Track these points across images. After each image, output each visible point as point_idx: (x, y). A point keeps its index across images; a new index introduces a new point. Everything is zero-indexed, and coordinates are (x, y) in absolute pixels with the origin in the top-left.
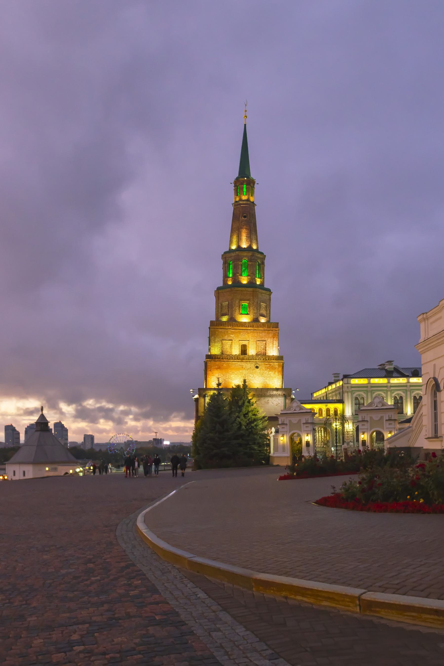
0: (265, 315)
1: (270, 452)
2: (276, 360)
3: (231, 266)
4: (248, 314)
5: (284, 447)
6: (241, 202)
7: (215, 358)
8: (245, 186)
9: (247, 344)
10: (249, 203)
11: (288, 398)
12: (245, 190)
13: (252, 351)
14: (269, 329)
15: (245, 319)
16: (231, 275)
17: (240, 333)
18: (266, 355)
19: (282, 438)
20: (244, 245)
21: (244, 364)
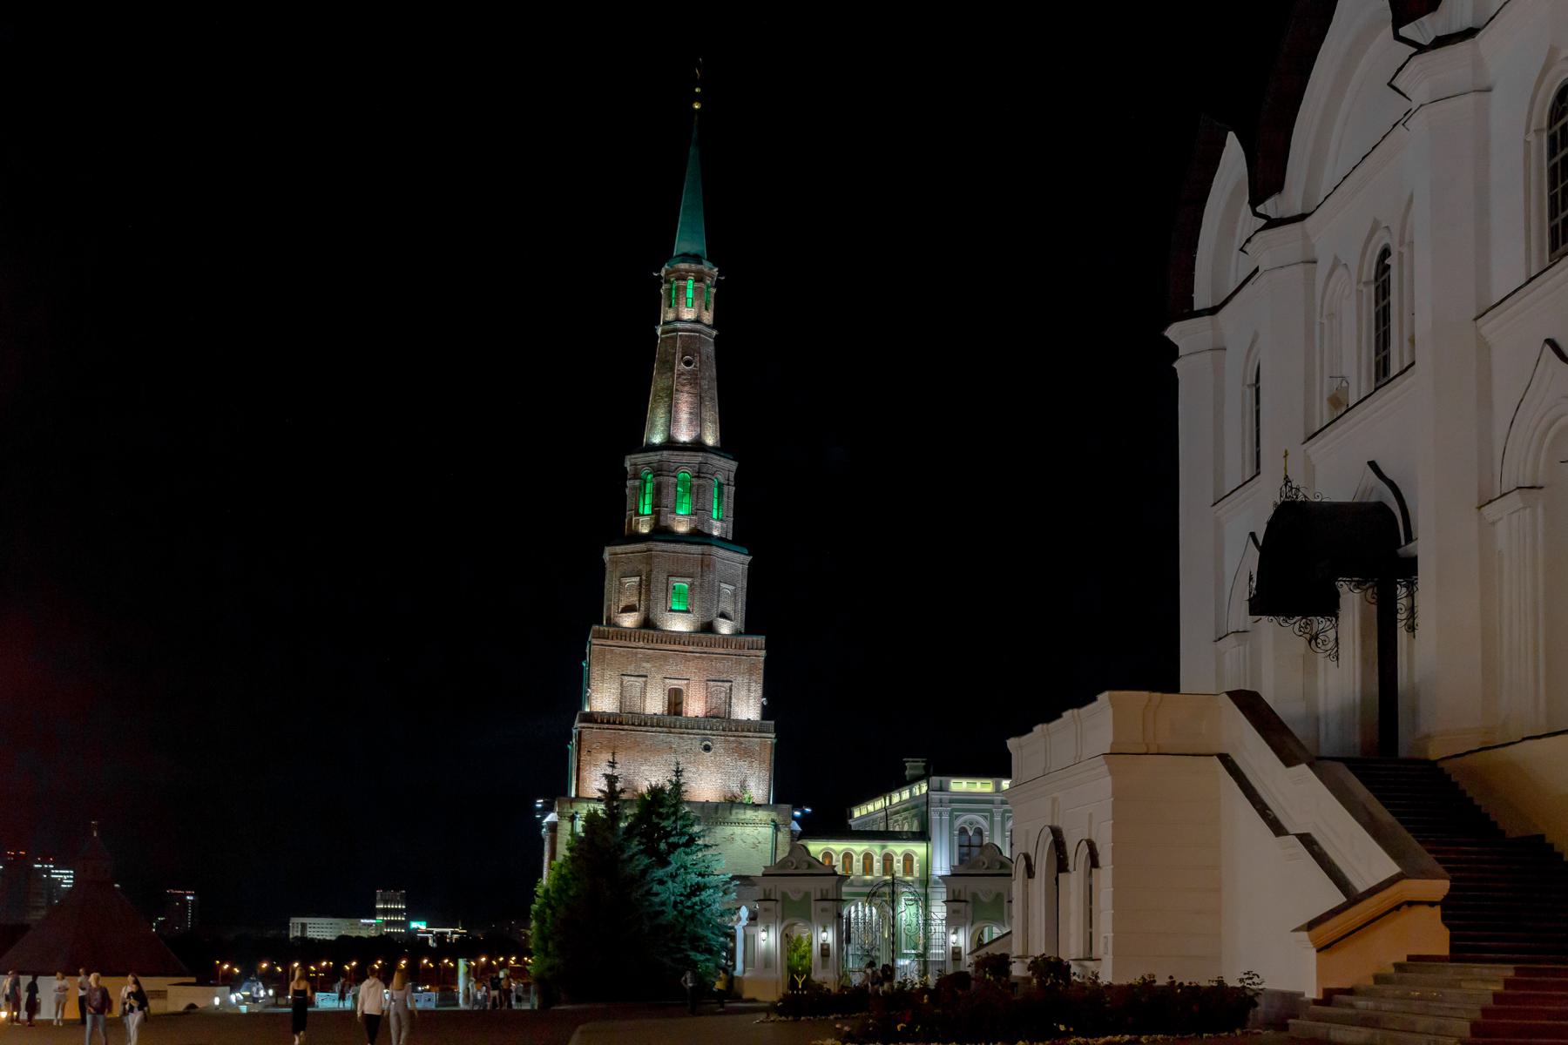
1: (734, 967)
3: (649, 487)
4: (687, 611)
6: (679, 325)
8: (690, 283)
9: (684, 689)
10: (698, 327)
12: (690, 293)
13: (695, 707)
15: (679, 624)
16: (648, 510)
17: (665, 658)
19: (764, 935)
20: (684, 436)
21: (673, 739)
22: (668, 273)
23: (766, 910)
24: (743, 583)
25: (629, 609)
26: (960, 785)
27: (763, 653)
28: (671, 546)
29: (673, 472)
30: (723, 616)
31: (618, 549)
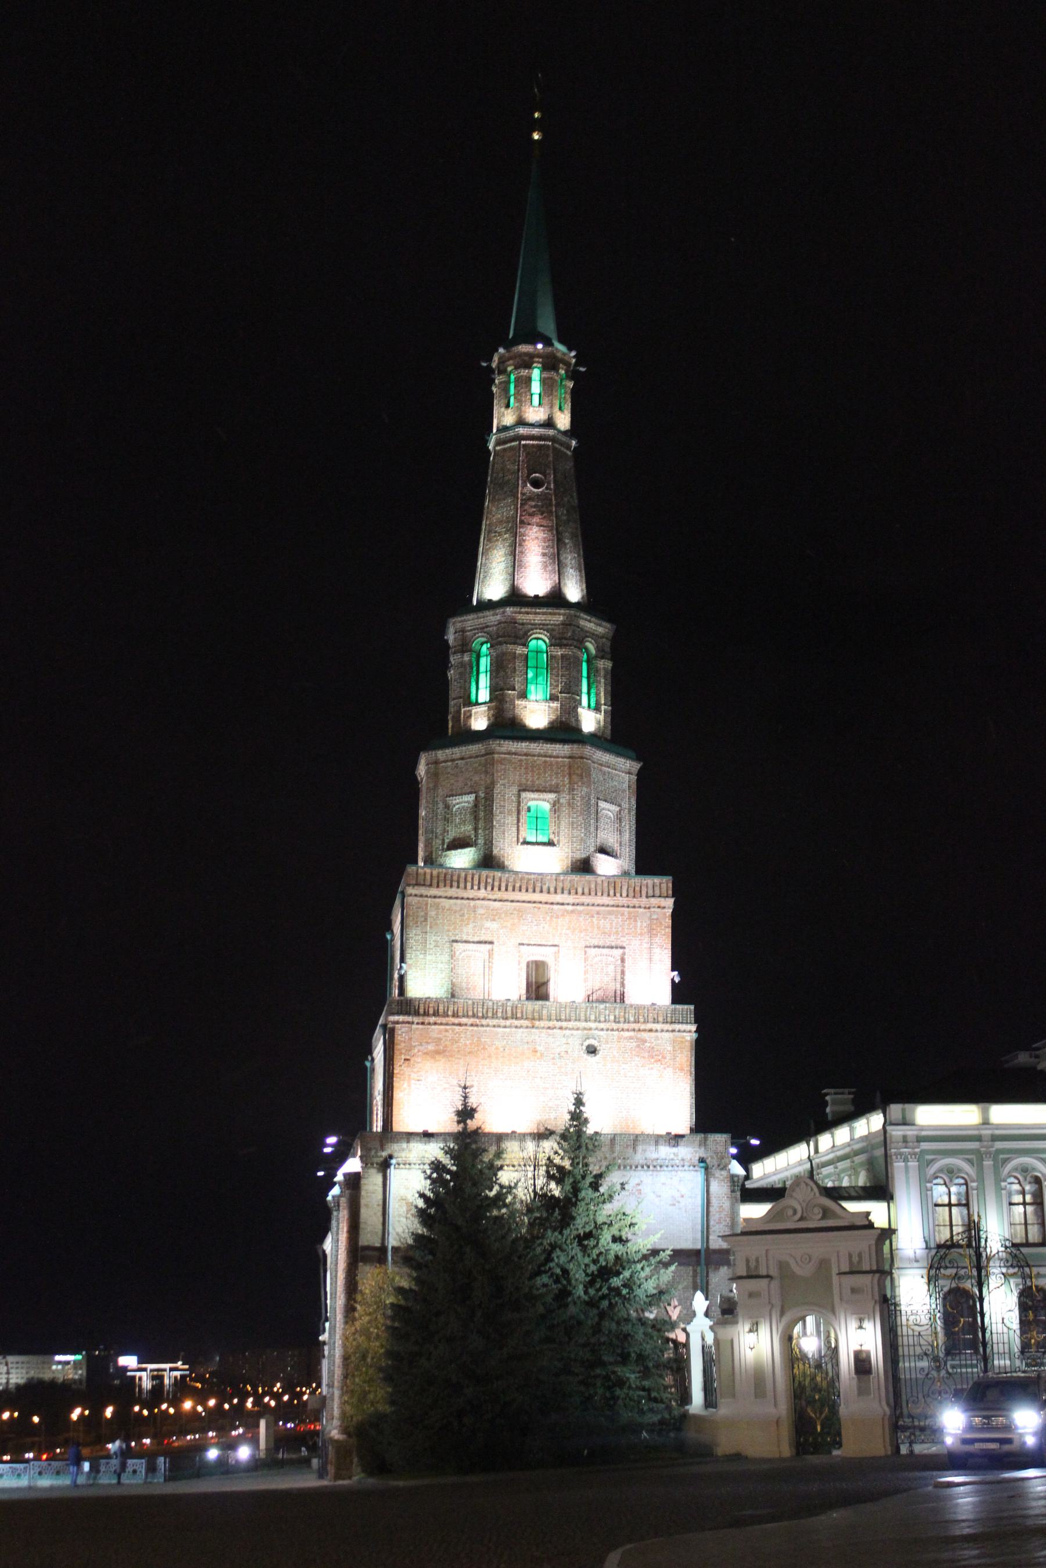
0: (616, 847)
1: (685, 1397)
2: (665, 1022)
3: (485, 663)
4: (551, 843)
5: (759, 1378)
6: (522, 431)
7: (426, 1014)
8: (536, 374)
10: (551, 432)
11: (718, 1173)
12: (536, 387)
13: (567, 987)
14: (635, 902)
16: (484, 695)
17: (521, 913)
18: (622, 1000)
21: (540, 1037)
22: (502, 361)
23: (751, 1295)
24: (629, 802)
25: (459, 844)
26: (931, 1116)
27: (670, 902)
28: (523, 746)
29: (522, 639)
30: (603, 850)
31: (441, 754)
